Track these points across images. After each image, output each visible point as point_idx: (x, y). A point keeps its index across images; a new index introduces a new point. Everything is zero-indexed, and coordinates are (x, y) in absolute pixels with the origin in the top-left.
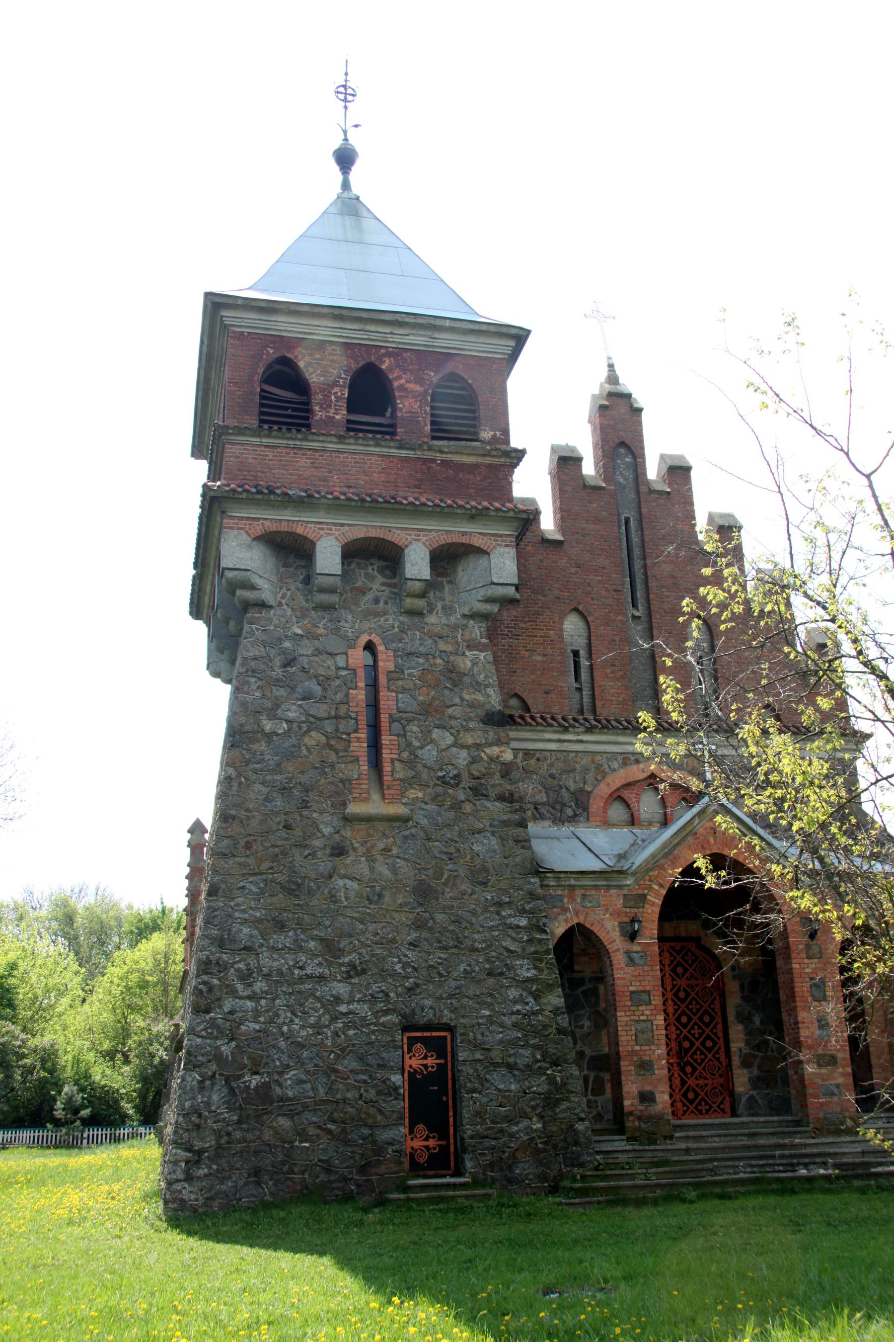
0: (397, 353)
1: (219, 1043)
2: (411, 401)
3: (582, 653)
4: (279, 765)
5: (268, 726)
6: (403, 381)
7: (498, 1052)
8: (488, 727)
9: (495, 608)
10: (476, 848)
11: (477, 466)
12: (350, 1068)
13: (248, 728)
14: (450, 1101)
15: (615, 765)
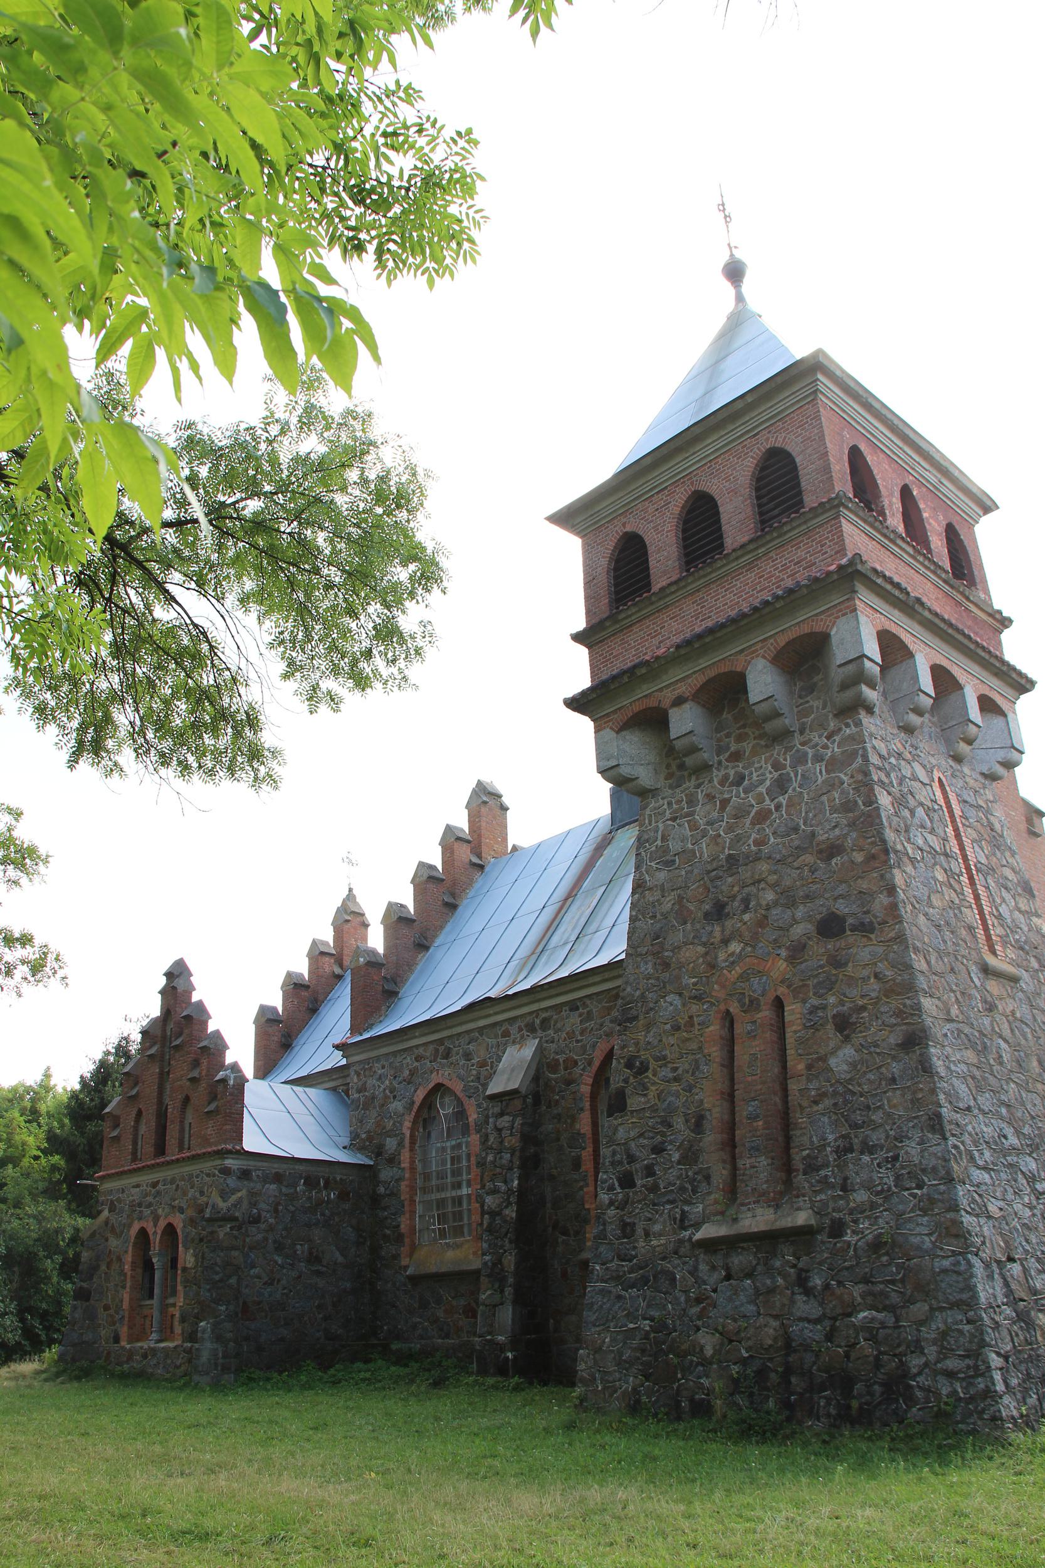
4: (929, 897)
13: (899, 847)
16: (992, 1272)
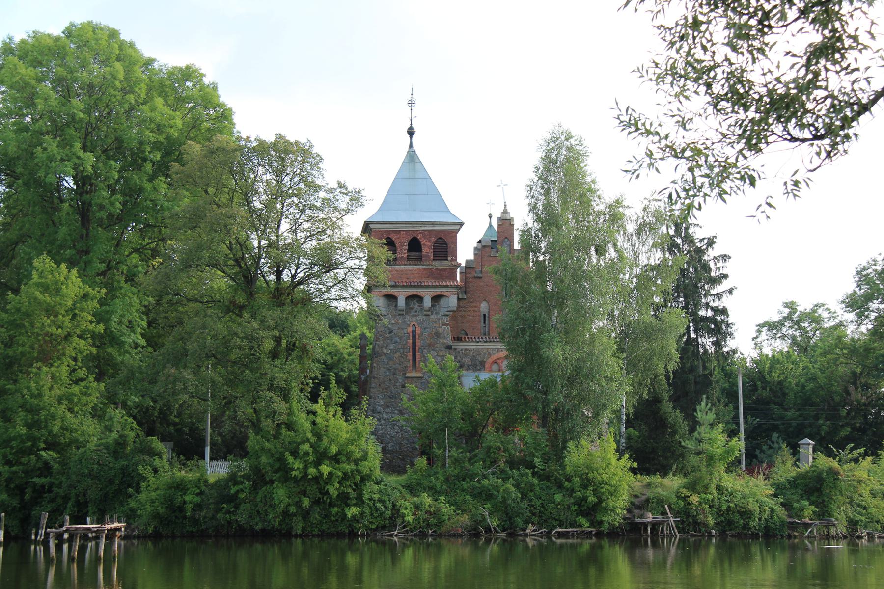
0: (423, 232)
5: (385, 351)
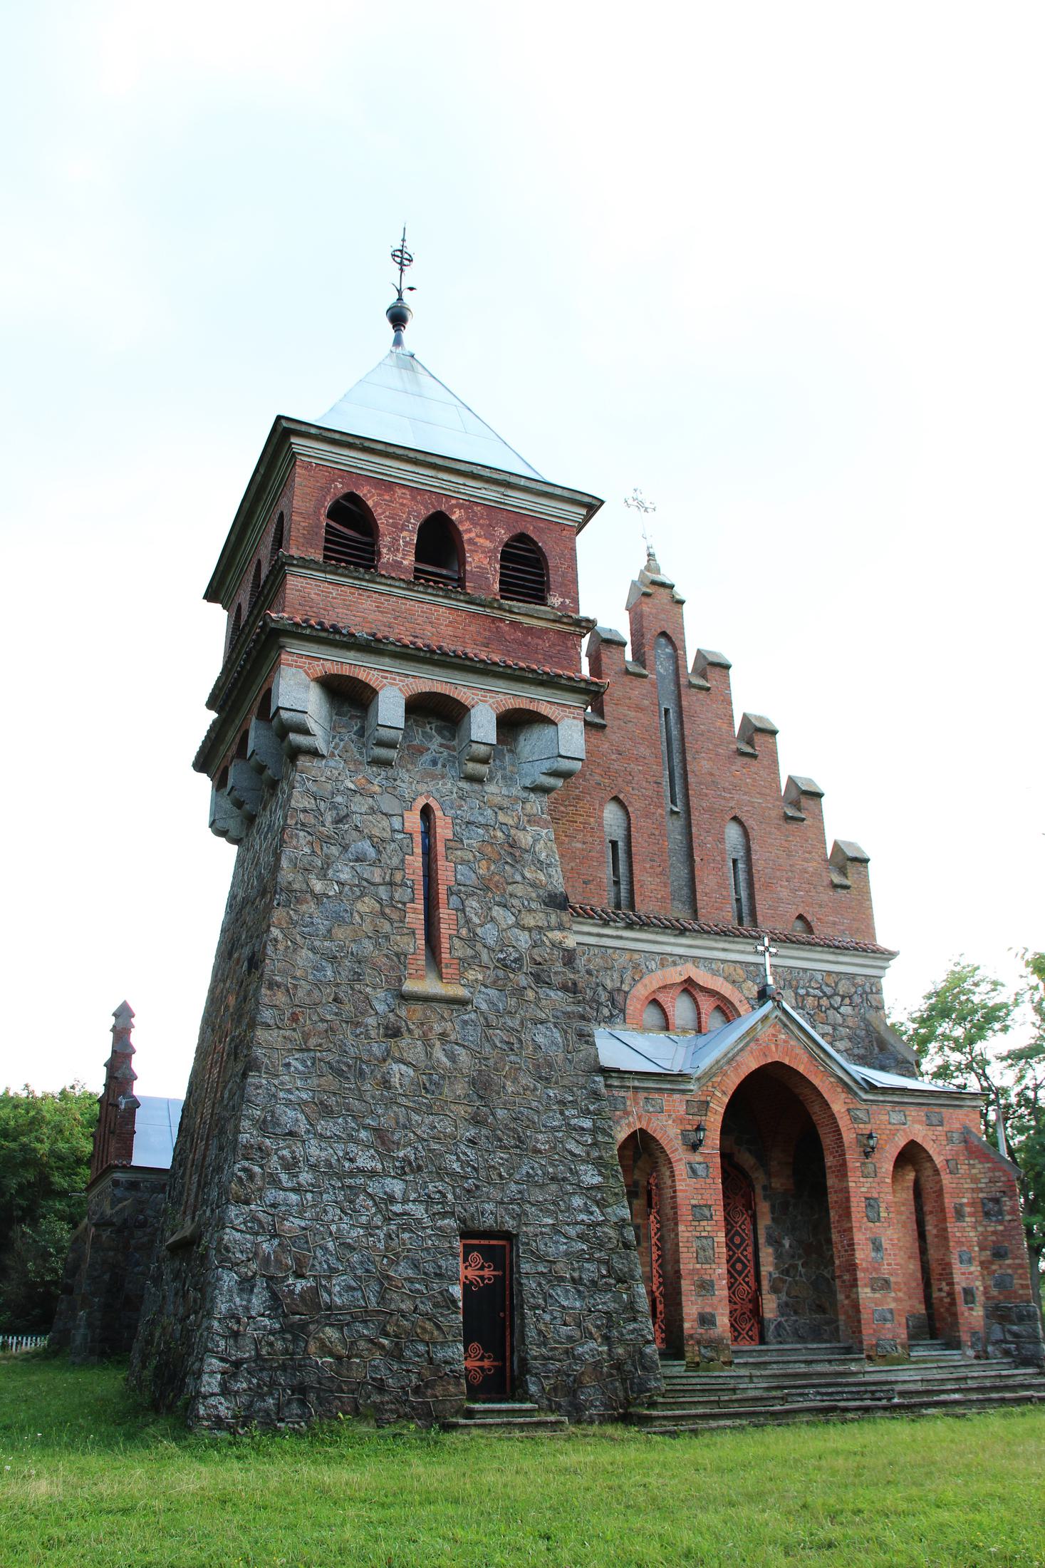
1: (260, 1239)
2: (482, 557)
3: (621, 844)
4: (329, 931)
5: (318, 886)
6: (473, 535)
7: (562, 1265)
8: (550, 910)
9: (559, 783)
10: (540, 1039)
11: (547, 631)
12: (405, 1276)
13: (296, 886)
14: (508, 1319)
15: (653, 965)
16: (253, 1286)
